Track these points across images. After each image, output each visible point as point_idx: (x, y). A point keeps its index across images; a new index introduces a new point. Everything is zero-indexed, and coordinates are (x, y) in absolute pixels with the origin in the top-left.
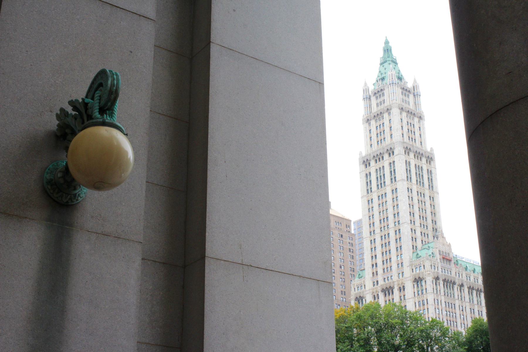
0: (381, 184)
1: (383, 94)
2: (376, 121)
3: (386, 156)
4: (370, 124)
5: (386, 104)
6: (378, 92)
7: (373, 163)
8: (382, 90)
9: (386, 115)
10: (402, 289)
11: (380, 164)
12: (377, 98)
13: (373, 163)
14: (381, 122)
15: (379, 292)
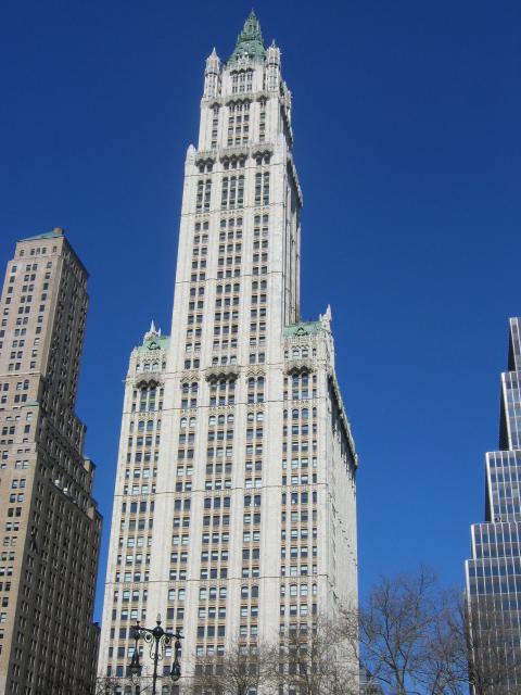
0: (232, 203)
1: (250, 77)
2: (232, 110)
3: (251, 162)
4: (216, 112)
5: (254, 91)
6: (242, 71)
7: (218, 166)
8: (250, 70)
9: (255, 107)
10: (257, 380)
11: (232, 172)
12: (235, 80)
13: (218, 166)
14: (243, 113)
15: (199, 380)
